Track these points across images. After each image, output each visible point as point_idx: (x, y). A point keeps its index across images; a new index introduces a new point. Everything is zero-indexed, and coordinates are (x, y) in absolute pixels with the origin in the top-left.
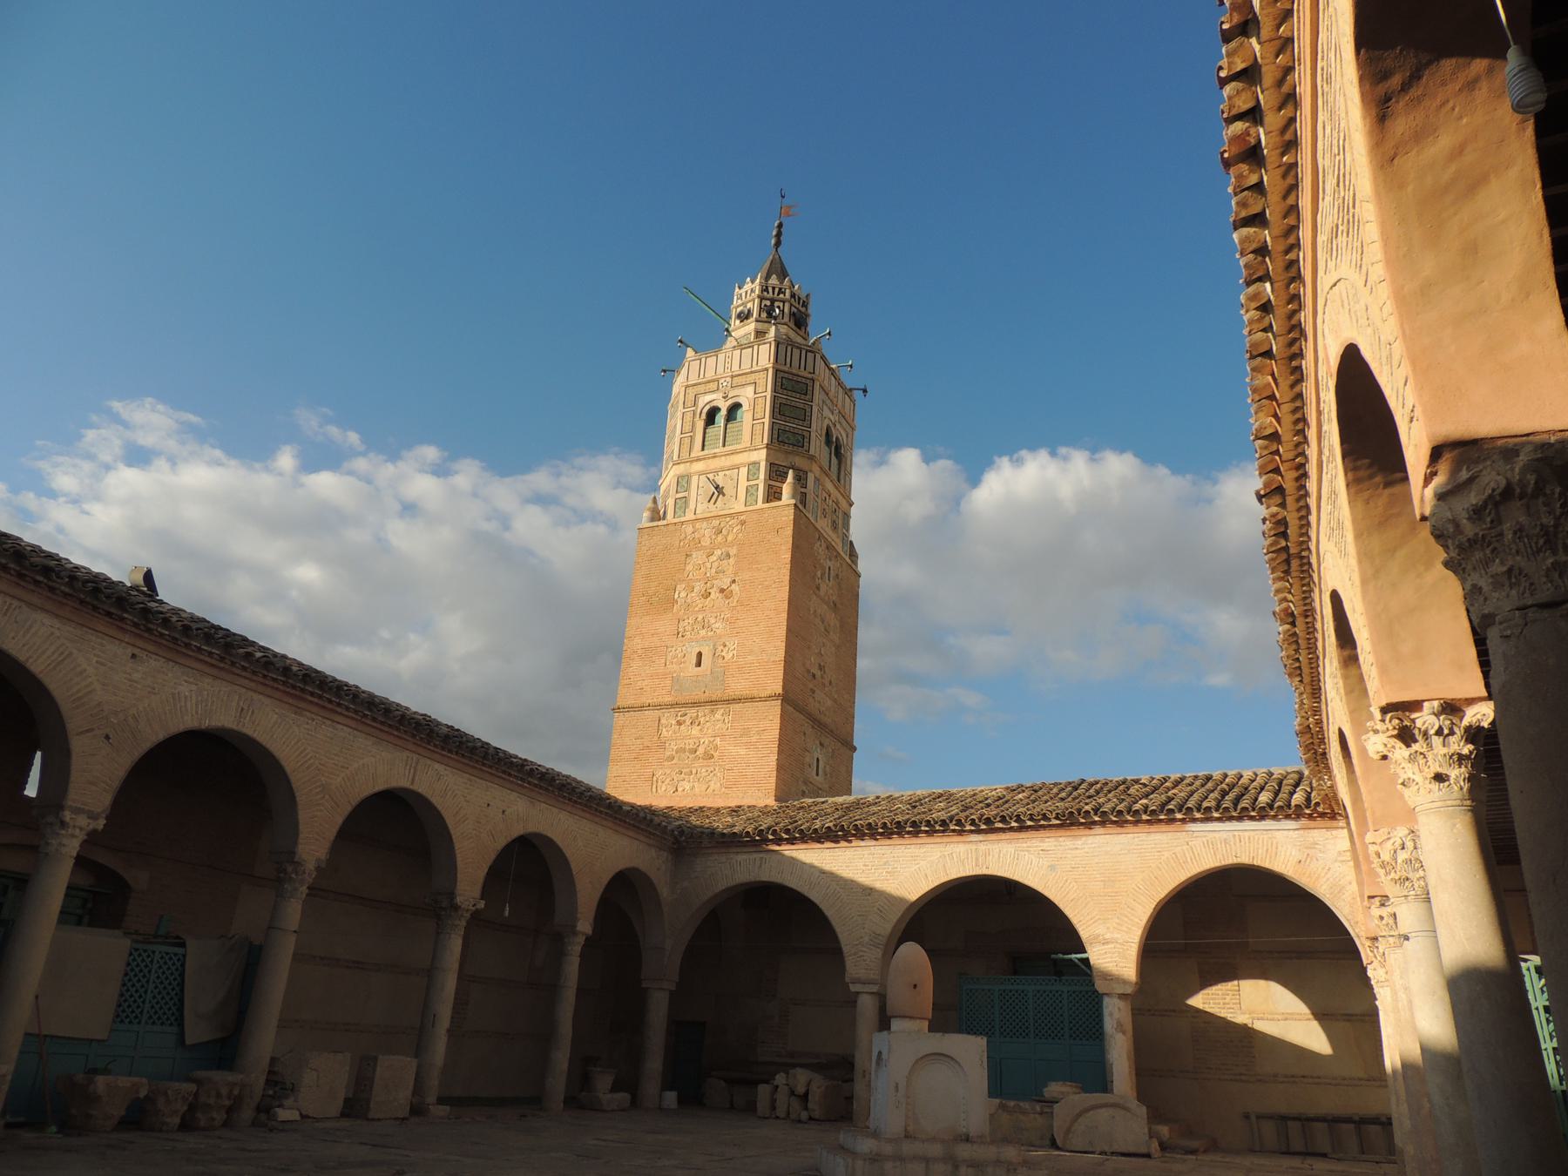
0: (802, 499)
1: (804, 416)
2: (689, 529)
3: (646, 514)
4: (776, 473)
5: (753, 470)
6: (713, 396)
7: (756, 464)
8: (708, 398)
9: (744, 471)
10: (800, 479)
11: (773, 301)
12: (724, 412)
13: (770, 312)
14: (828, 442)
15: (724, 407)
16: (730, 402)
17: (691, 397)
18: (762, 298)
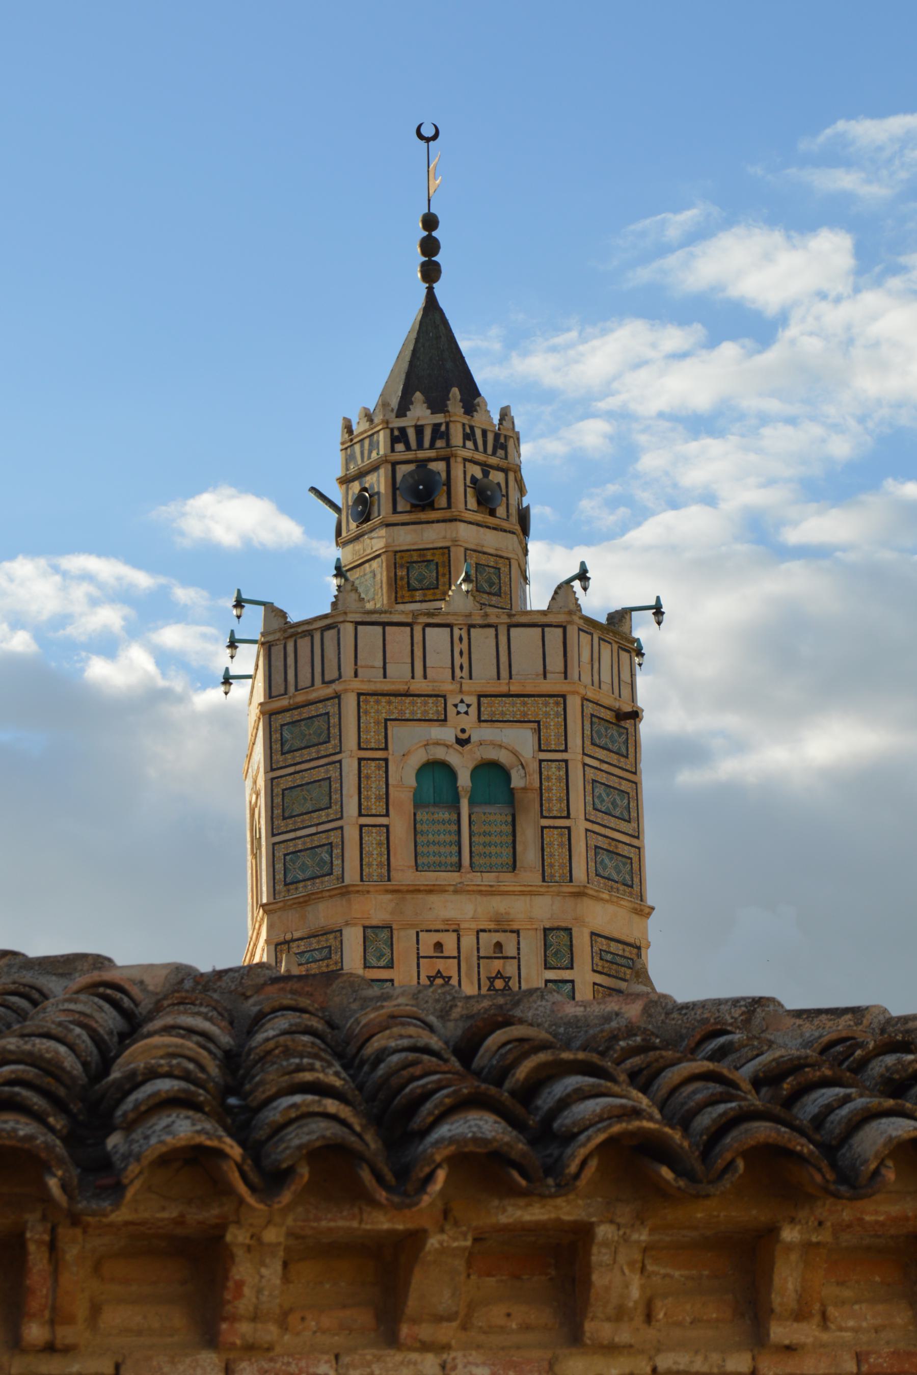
6: (437, 732)
11: (486, 468)
15: (463, 765)
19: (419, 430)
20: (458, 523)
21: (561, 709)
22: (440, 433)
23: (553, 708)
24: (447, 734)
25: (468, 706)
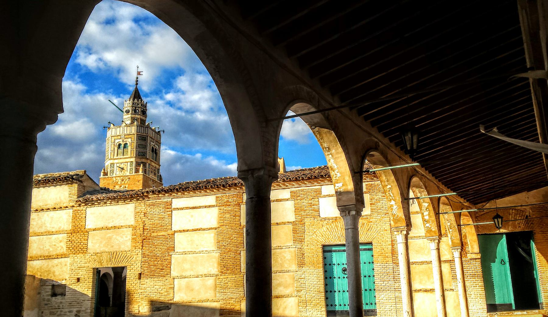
0: (145, 171)
1: (145, 147)
2: (115, 179)
3: (102, 174)
4: (138, 164)
8: (118, 141)
9: (129, 163)
10: (145, 165)
11: (136, 107)
12: (122, 146)
13: (135, 111)
14: (153, 151)
15: (123, 144)
17: (113, 140)
18: (132, 107)
24: (121, 140)
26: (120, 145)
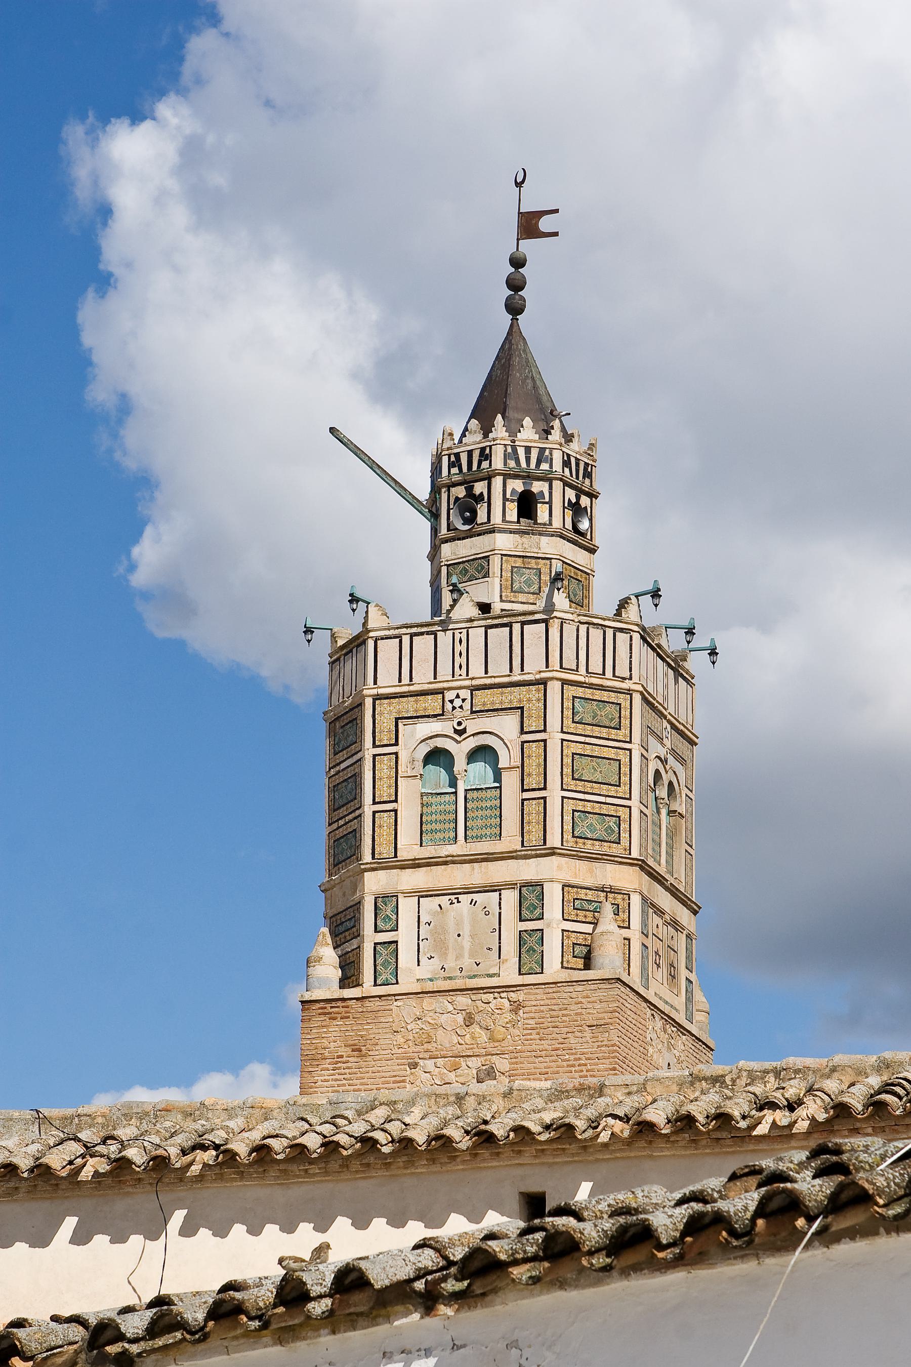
5: (532, 898)
6: (435, 727)
7: (537, 886)
9: (510, 898)
16: (471, 744)
17: (386, 723)
19: (470, 453)
20: (497, 535)
21: (541, 695)
22: (485, 455)
23: (534, 693)
25: (464, 700)
26: (437, 757)
